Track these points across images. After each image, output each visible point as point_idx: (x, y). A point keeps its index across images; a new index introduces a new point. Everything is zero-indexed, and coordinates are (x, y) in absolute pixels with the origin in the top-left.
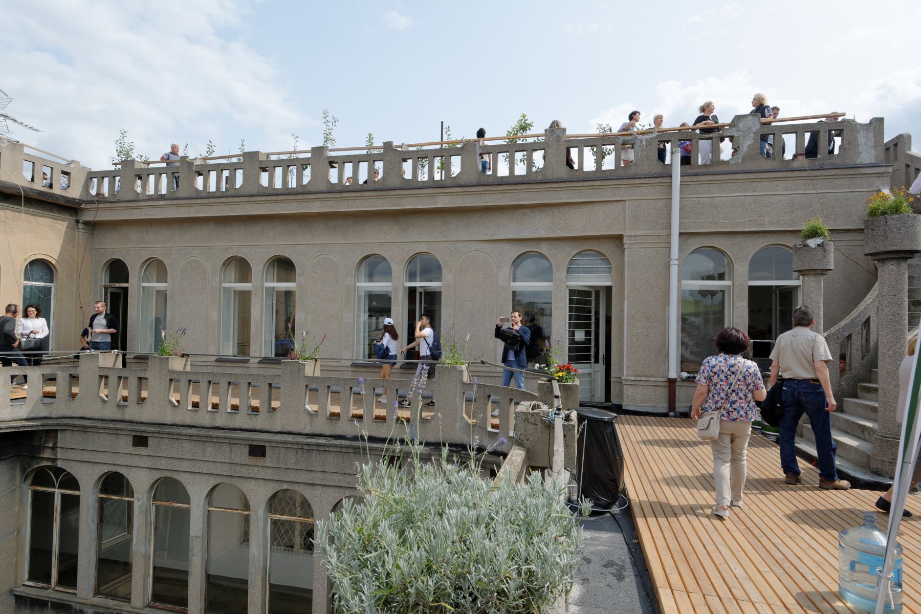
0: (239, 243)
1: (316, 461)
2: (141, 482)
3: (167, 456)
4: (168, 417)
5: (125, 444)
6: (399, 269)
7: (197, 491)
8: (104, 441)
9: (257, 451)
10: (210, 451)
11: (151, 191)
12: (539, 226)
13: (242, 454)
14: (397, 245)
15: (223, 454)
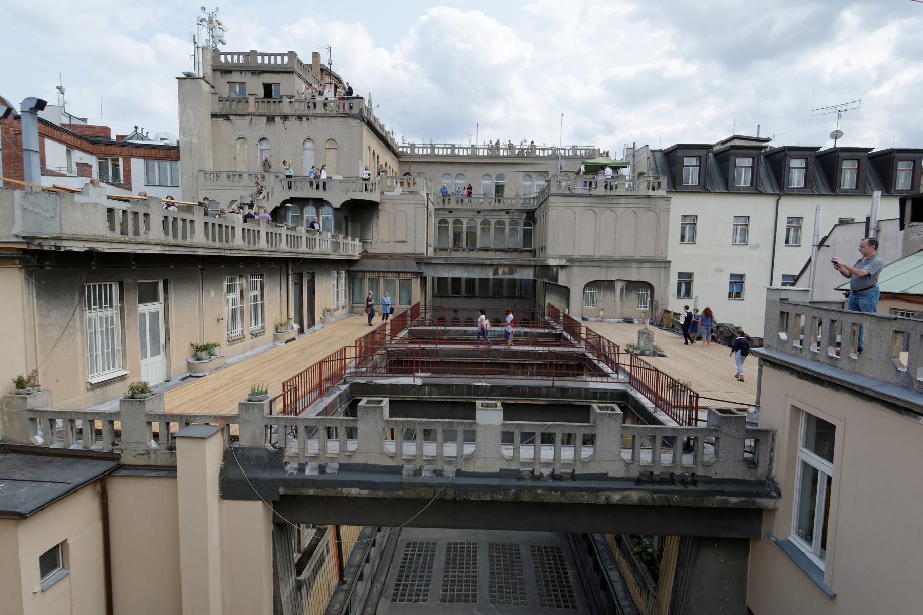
0: (447, 169)
1: (492, 213)
2: (451, 221)
3: (457, 215)
4: (456, 207)
5: (447, 213)
6: (494, 178)
7: (465, 222)
8: (441, 212)
9: (479, 212)
10: (468, 213)
11: (421, 153)
12: (530, 168)
13: (475, 213)
14: (494, 171)
15: (471, 213)
